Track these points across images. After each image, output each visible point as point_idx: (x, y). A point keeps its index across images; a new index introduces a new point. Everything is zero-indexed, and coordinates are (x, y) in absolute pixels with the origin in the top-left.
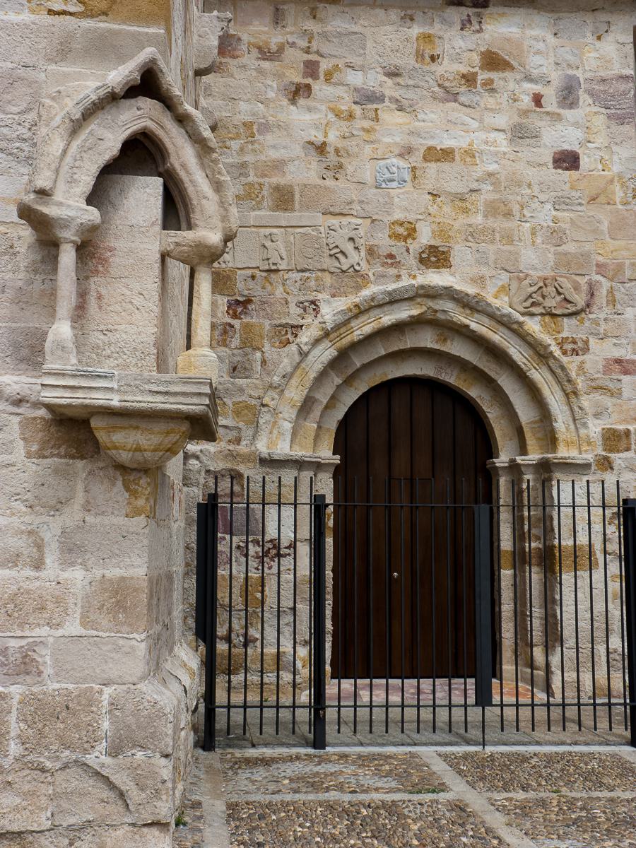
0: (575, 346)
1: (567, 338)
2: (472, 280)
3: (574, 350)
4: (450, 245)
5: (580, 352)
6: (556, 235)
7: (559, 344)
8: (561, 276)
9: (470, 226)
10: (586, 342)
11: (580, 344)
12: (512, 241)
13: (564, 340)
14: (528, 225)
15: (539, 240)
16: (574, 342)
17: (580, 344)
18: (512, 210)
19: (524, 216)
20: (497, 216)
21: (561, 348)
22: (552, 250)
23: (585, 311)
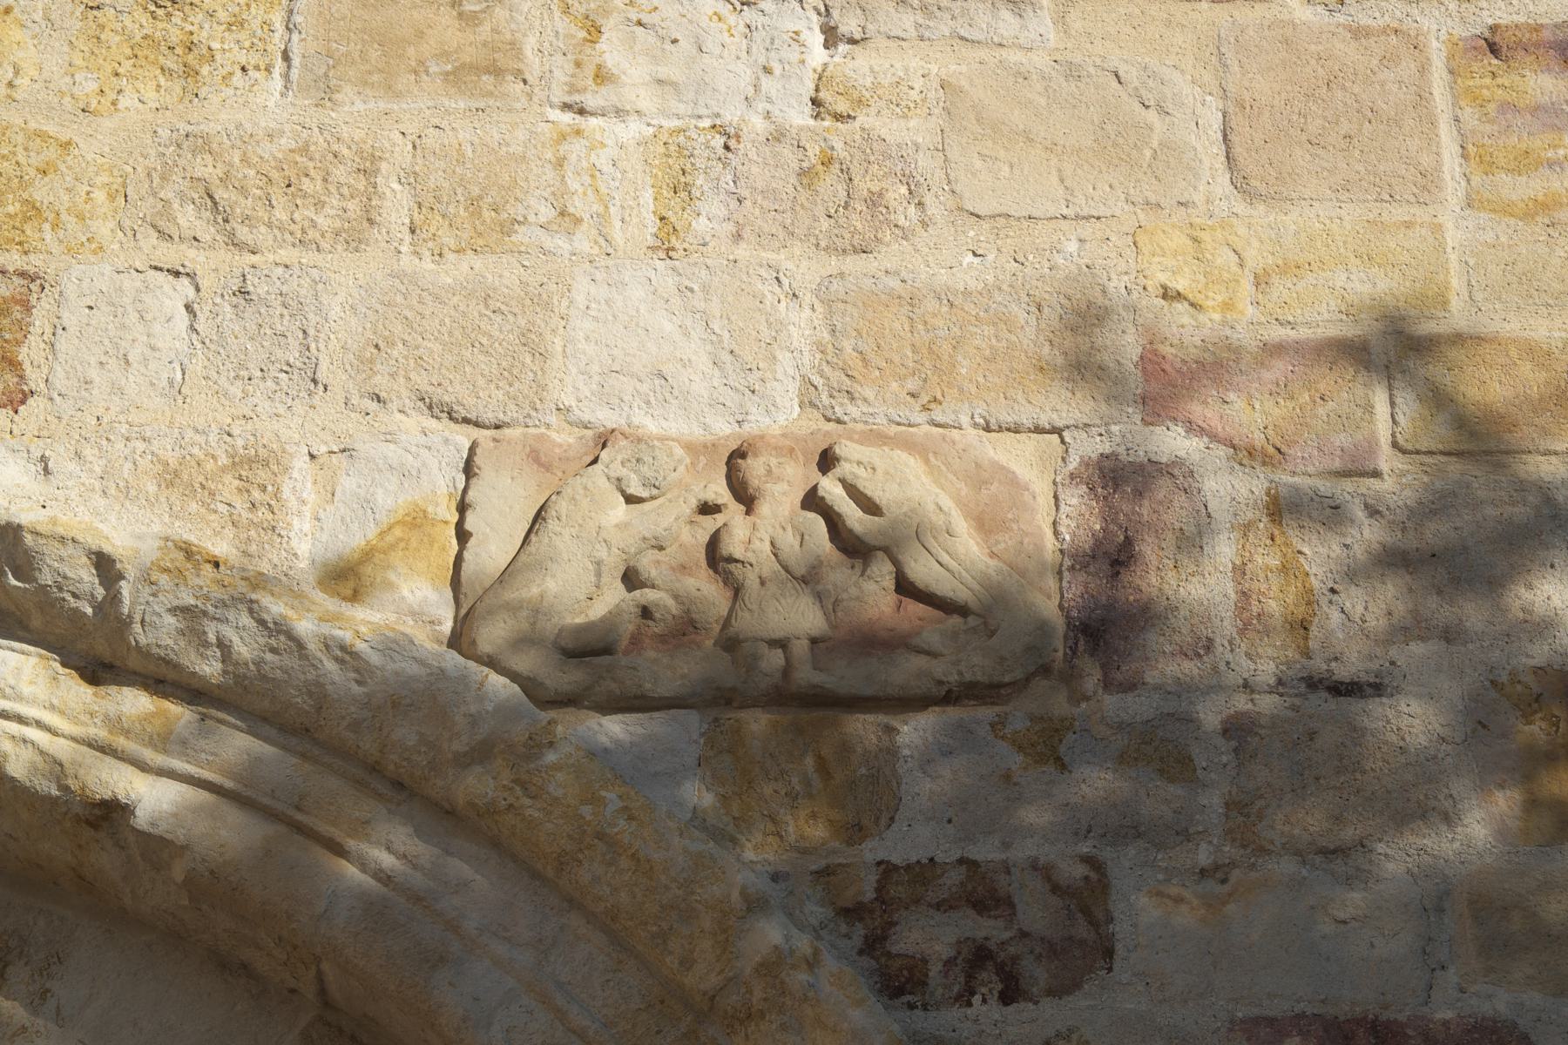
0: (989, 929)
1: (924, 872)
2: (170, 477)
3: (979, 956)
4: (35, 262)
5: (1036, 973)
6: (840, 186)
7: (853, 913)
8: (876, 438)
9: (203, 145)
10: (1088, 899)
11: (1036, 912)
12: (508, 227)
13: (906, 884)
14: (633, 130)
15: (708, 219)
16: (983, 893)
17: (1036, 912)
18: (515, 48)
19: (602, 76)
20: (405, 80)
21: (873, 945)
22: (805, 268)
23: (1070, 677)
